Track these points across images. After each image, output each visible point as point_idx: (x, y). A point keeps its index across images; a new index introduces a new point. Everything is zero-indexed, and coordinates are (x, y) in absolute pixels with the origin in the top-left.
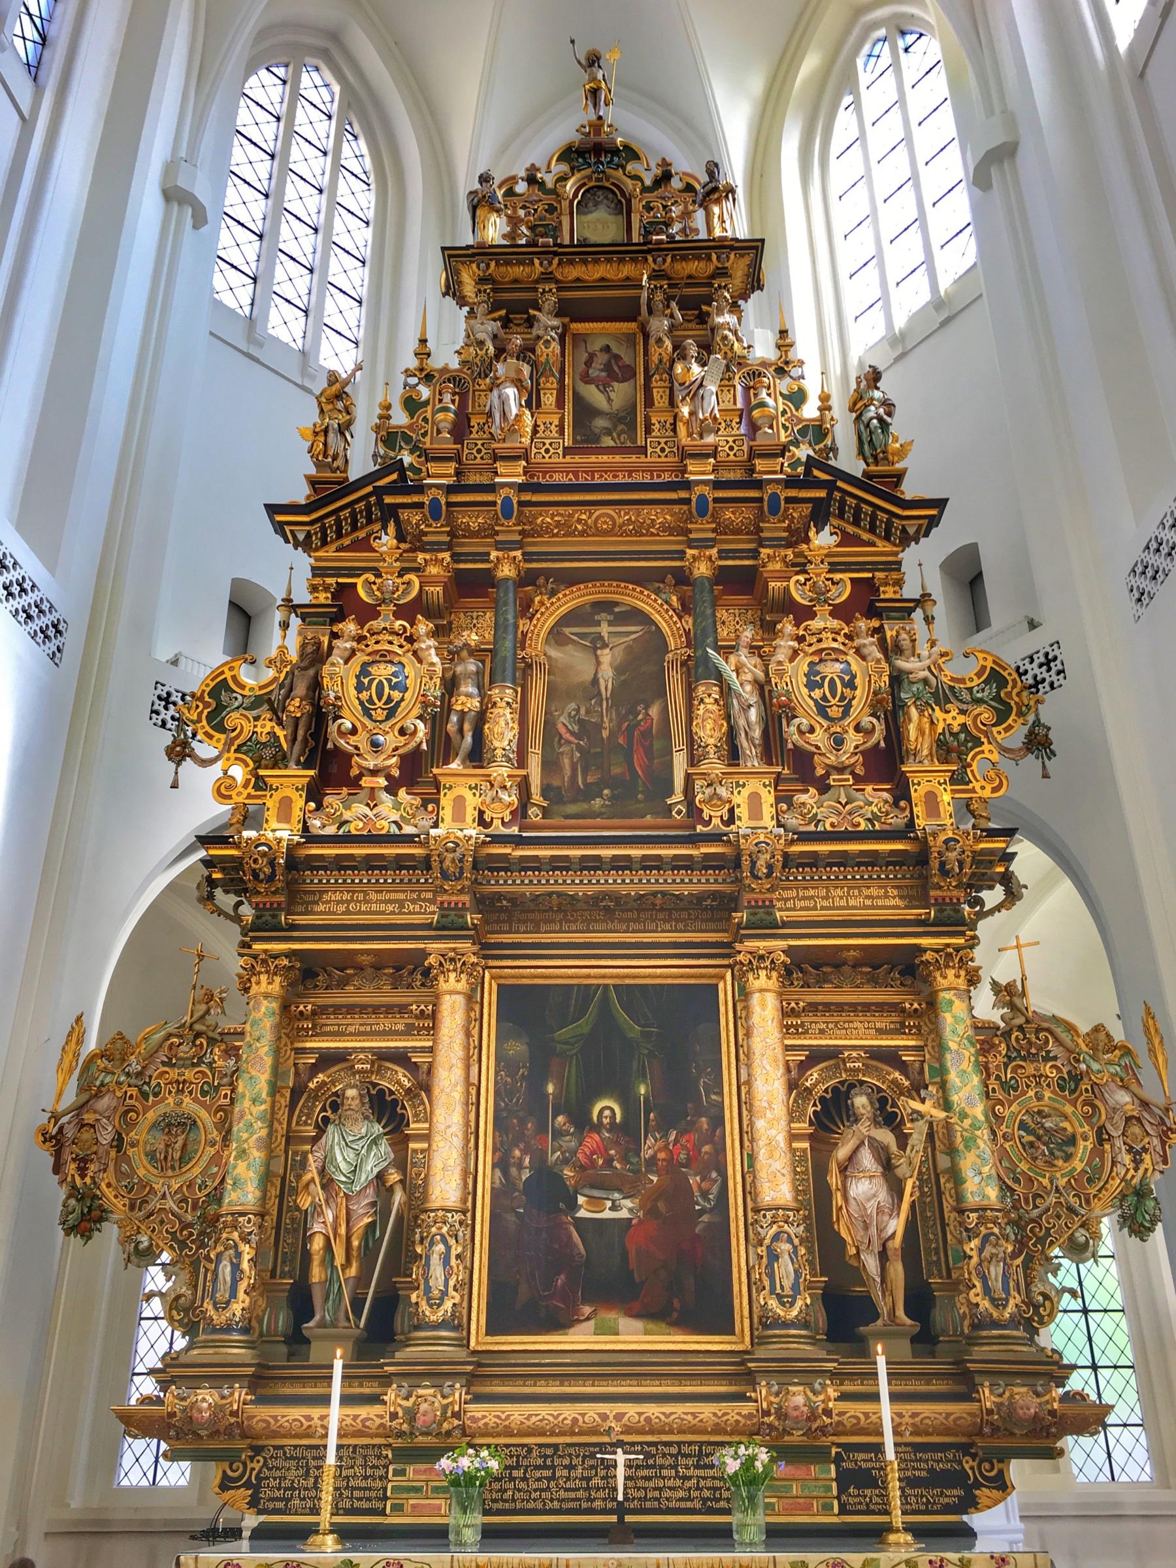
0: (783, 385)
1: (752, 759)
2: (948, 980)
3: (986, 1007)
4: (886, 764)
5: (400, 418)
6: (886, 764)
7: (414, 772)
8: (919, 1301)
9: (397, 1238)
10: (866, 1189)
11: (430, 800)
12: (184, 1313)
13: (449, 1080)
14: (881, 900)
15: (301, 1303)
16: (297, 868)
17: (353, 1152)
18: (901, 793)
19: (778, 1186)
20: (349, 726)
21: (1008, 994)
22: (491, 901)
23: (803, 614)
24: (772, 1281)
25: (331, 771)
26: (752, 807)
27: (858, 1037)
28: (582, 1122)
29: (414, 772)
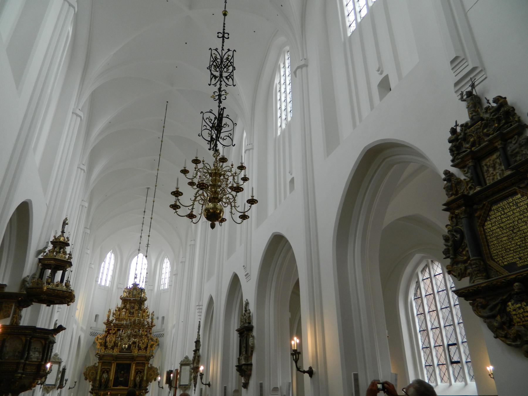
1: (137, 348)
2: (146, 365)
3: (149, 366)
4: (146, 348)
5: (115, 312)
7: (113, 348)
8: (140, 385)
10: (138, 378)
11: (113, 349)
12: (92, 385)
13: (112, 371)
16: (103, 356)
17: (105, 376)
18: (146, 350)
19: (132, 379)
20: (108, 344)
21: (151, 365)
22: (116, 358)
24: (131, 384)
25: (106, 347)
29: (113, 348)
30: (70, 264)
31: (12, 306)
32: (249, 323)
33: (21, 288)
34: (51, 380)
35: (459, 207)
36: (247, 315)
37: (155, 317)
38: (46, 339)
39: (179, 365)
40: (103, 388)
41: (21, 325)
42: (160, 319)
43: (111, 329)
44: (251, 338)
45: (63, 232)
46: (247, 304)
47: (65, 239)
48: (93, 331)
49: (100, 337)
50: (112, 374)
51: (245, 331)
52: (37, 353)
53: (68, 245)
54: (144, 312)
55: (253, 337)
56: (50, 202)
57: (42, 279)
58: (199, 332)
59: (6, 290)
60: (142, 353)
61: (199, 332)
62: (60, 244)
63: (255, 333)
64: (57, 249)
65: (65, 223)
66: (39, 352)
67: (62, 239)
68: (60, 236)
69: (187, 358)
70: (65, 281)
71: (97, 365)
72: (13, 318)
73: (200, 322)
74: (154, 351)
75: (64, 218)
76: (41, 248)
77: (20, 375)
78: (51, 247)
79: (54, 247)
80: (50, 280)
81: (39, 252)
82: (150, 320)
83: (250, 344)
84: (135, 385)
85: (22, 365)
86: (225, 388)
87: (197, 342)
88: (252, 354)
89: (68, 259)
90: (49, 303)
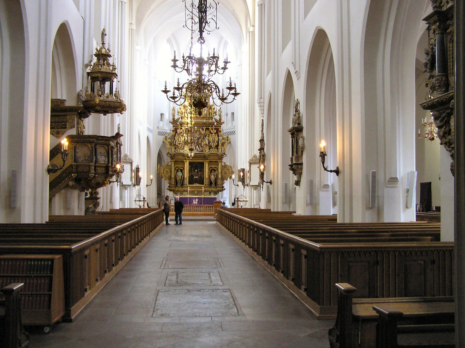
0: (213, 107)
4: (217, 146)
6: (217, 146)
8: (216, 183)
9: (183, 179)
12: (170, 184)
14: (216, 157)
15: (177, 183)
17: (180, 174)
18: (218, 149)
19: (207, 177)
21: (224, 163)
23: (212, 134)
24: (206, 182)
26: (207, 151)
27: (213, 166)
28: (194, 171)
30: (116, 75)
31: (74, 118)
32: (299, 124)
33: (78, 102)
34: (126, 178)
35: (435, 23)
36: (297, 116)
37: (223, 114)
38: (108, 145)
39: (248, 164)
40: (179, 186)
41: (86, 133)
42: (230, 115)
43: (178, 129)
44: (301, 139)
45: (103, 44)
46: (298, 103)
47: (106, 50)
48: (161, 131)
49: (169, 137)
50: (186, 172)
51: (296, 131)
52: (103, 157)
53: (110, 56)
54: (211, 108)
55: (303, 138)
56: (85, 12)
57: (94, 92)
58: (262, 131)
59: (67, 104)
60: (213, 151)
61: (262, 131)
62: (103, 56)
63: (304, 133)
64: (101, 62)
65: (103, 35)
66: (105, 156)
67: (103, 51)
68: (101, 48)
69: (255, 156)
70: (114, 93)
71: (170, 164)
72: (78, 128)
73: (263, 120)
74: (227, 149)
75: (102, 29)
76: (86, 62)
77: (93, 175)
78: (95, 59)
79: (99, 59)
80: (100, 93)
81: (87, 66)
82: (217, 117)
83: (300, 144)
84: (211, 183)
85: (93, 167)
86: (286, 185)
87: (262, 141)
88: (302, 154)
89: (112, 71)
90: (105, 113)
